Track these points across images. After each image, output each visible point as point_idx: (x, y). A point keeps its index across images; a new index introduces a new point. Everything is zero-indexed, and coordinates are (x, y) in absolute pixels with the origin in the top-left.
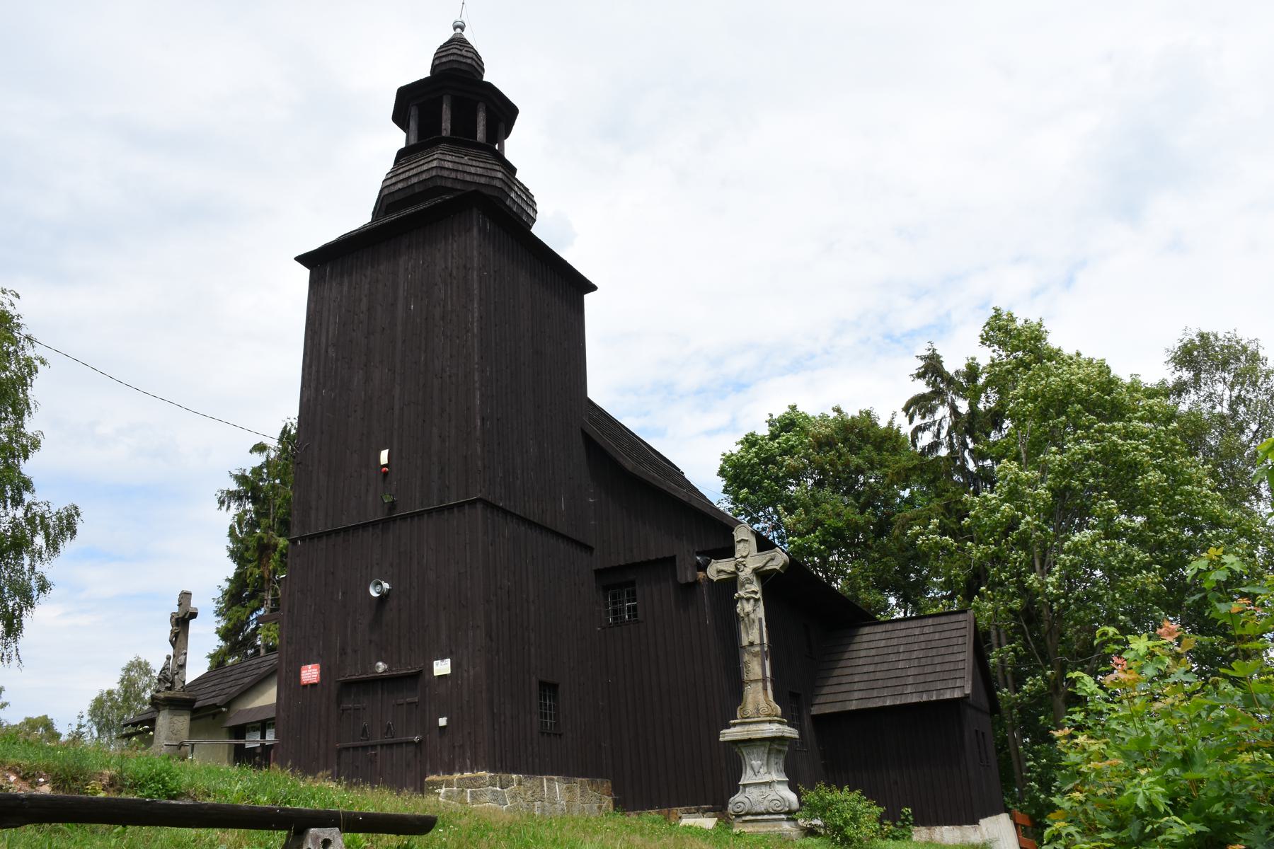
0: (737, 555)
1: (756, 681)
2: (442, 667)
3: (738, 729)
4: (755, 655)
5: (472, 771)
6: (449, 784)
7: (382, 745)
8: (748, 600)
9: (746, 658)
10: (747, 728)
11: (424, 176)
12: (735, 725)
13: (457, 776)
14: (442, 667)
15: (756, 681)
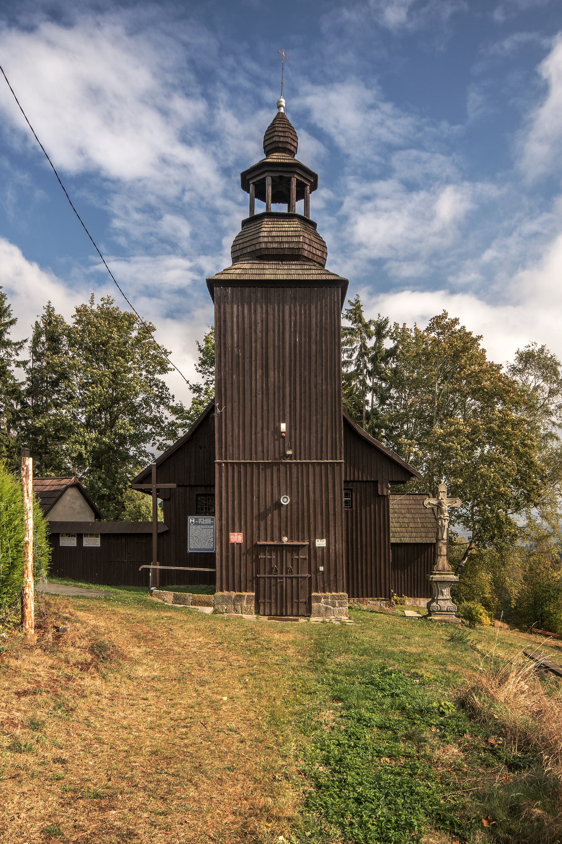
0: (440, 498)
1: (444, 555)
2: (321, 543)
3: (437, 576)
4: (444, 544)
5: (336, 592)
6: (325, 597)
7: (286, 578)
8: (445, 520)
9: (440, 545)
10: (443, 576)
11: (292, 246)
12: (435, 574)
13: (328, 594)
14: (321, 543)
15: (444, 555)
